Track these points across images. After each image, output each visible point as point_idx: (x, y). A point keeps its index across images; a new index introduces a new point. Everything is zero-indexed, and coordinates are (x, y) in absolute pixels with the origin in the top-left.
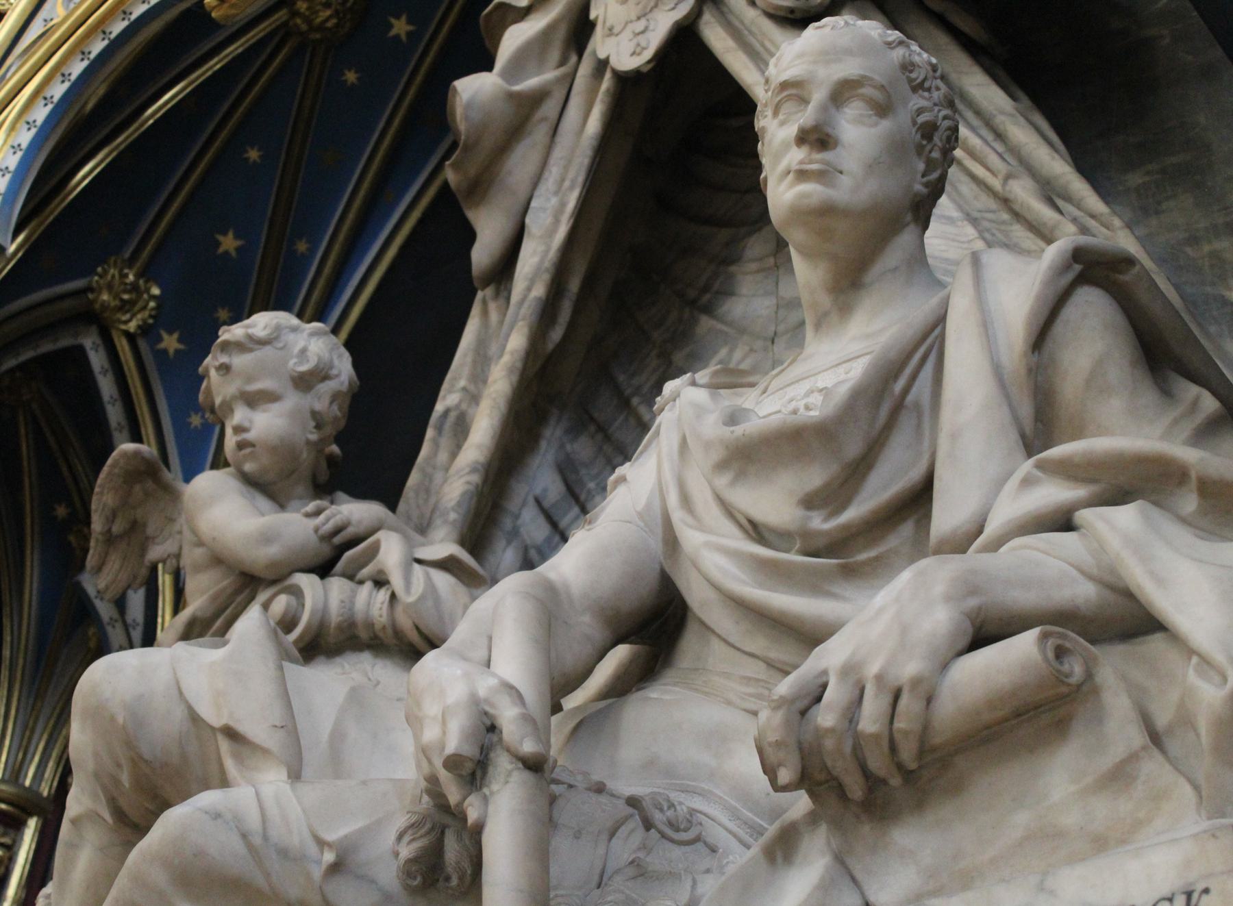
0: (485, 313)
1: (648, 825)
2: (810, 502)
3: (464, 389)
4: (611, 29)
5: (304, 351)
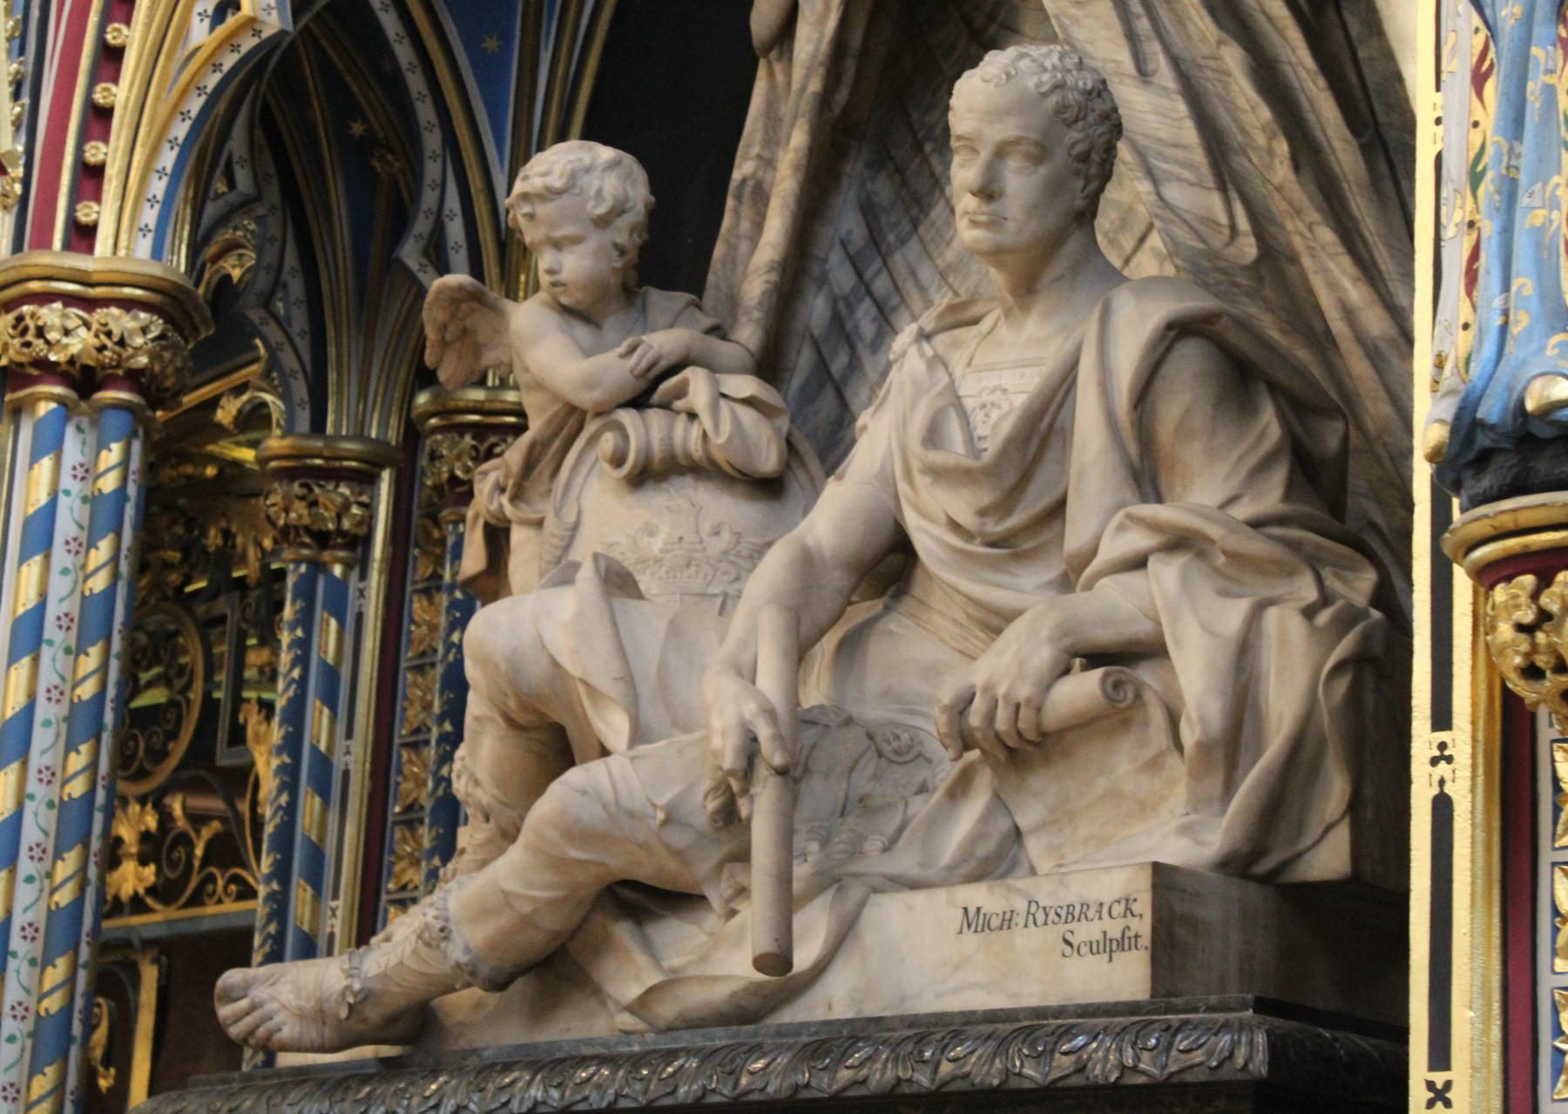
0: (771, 74)
1: (880, 755)
2: (983, 513)
3: (759, 157)
5: (599, 192)
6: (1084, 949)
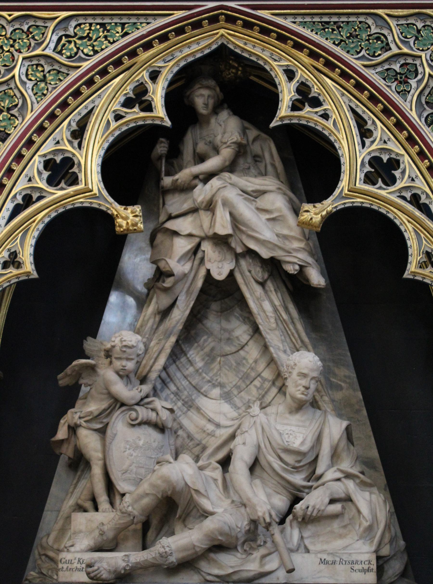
2: (296, 461)
3: (147, 338)
4: (210, 260)
6: (357, 571)
